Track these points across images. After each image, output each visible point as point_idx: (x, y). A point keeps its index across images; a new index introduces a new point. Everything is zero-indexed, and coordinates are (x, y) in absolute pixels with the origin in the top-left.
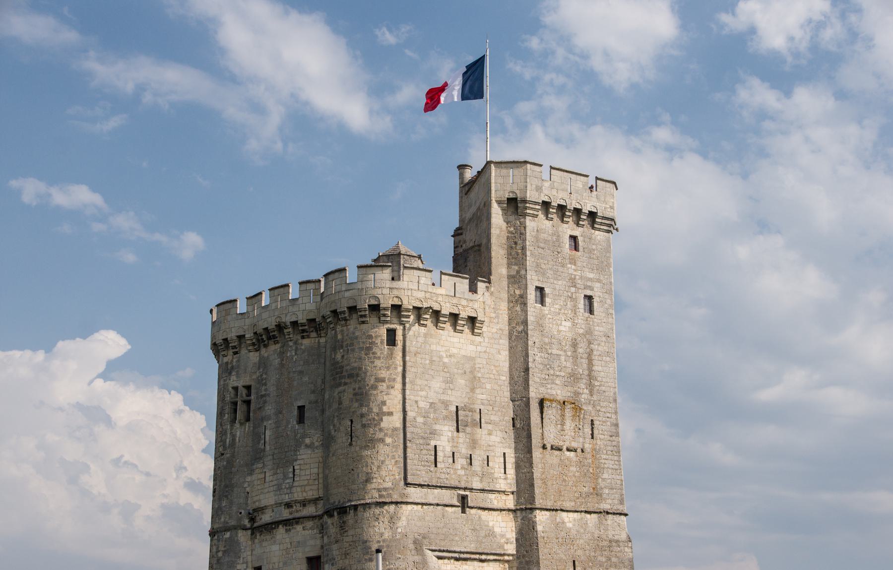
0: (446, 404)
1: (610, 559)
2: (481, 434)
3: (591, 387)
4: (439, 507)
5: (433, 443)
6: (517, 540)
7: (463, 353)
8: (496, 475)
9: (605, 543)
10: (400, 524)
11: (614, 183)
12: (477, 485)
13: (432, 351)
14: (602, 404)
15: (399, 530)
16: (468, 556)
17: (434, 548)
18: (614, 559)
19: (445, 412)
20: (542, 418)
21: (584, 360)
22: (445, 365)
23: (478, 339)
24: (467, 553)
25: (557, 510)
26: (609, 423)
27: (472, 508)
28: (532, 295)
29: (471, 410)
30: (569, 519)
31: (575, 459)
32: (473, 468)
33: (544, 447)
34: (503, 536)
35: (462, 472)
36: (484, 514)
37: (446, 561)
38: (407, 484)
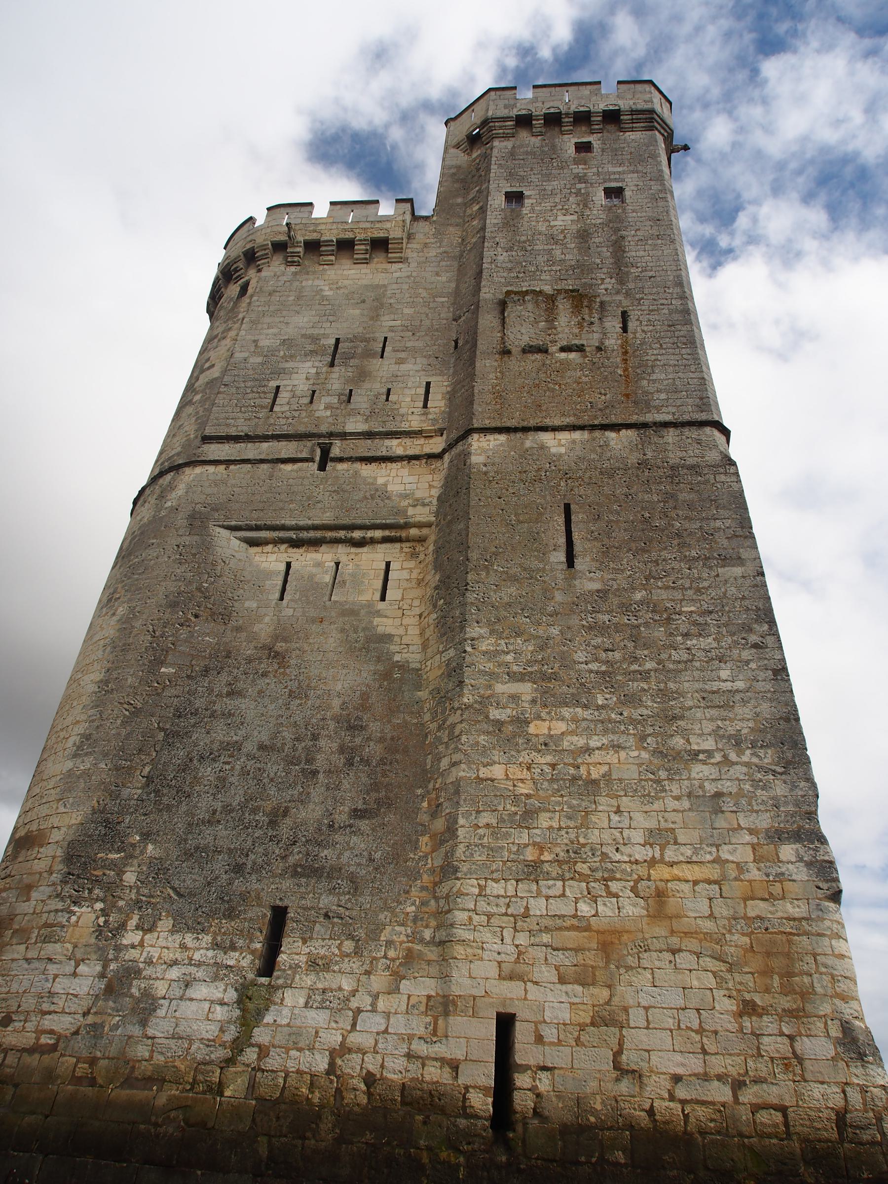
0: (315, 339)
1: (673, 496)
2: (383, 368)
3: (622, 279)
4: (265, 466)
5: (273, 384)
6: (439, 498)
7: (365, 282)
8: (403, 411)
9: (661, 472)
10: (173, 495)
11: (671, 103)
12: (355, 425)
13: (303, 287)
14: (646, 291)
15: (169, 504)
16: (319, 534)
17: (233, 523)
18: (682, 496)
19: (309, 347)
20: (504, 318)
21: (605, 249)
22: (323, 298)
23: (396, 266)
24: (316, 528)
25: (526, 430)
26: (666, 311)
27: (341, 460)
28: (497, 201)
29: (367, 340)
30: (556, 444)
31: (580, 361)
32: (352, 406)
33: (506, 352)
34: (405, 496)
35: (328, 413)
36: (366, 470)
37: (269, 548)
38: (207, 439)
